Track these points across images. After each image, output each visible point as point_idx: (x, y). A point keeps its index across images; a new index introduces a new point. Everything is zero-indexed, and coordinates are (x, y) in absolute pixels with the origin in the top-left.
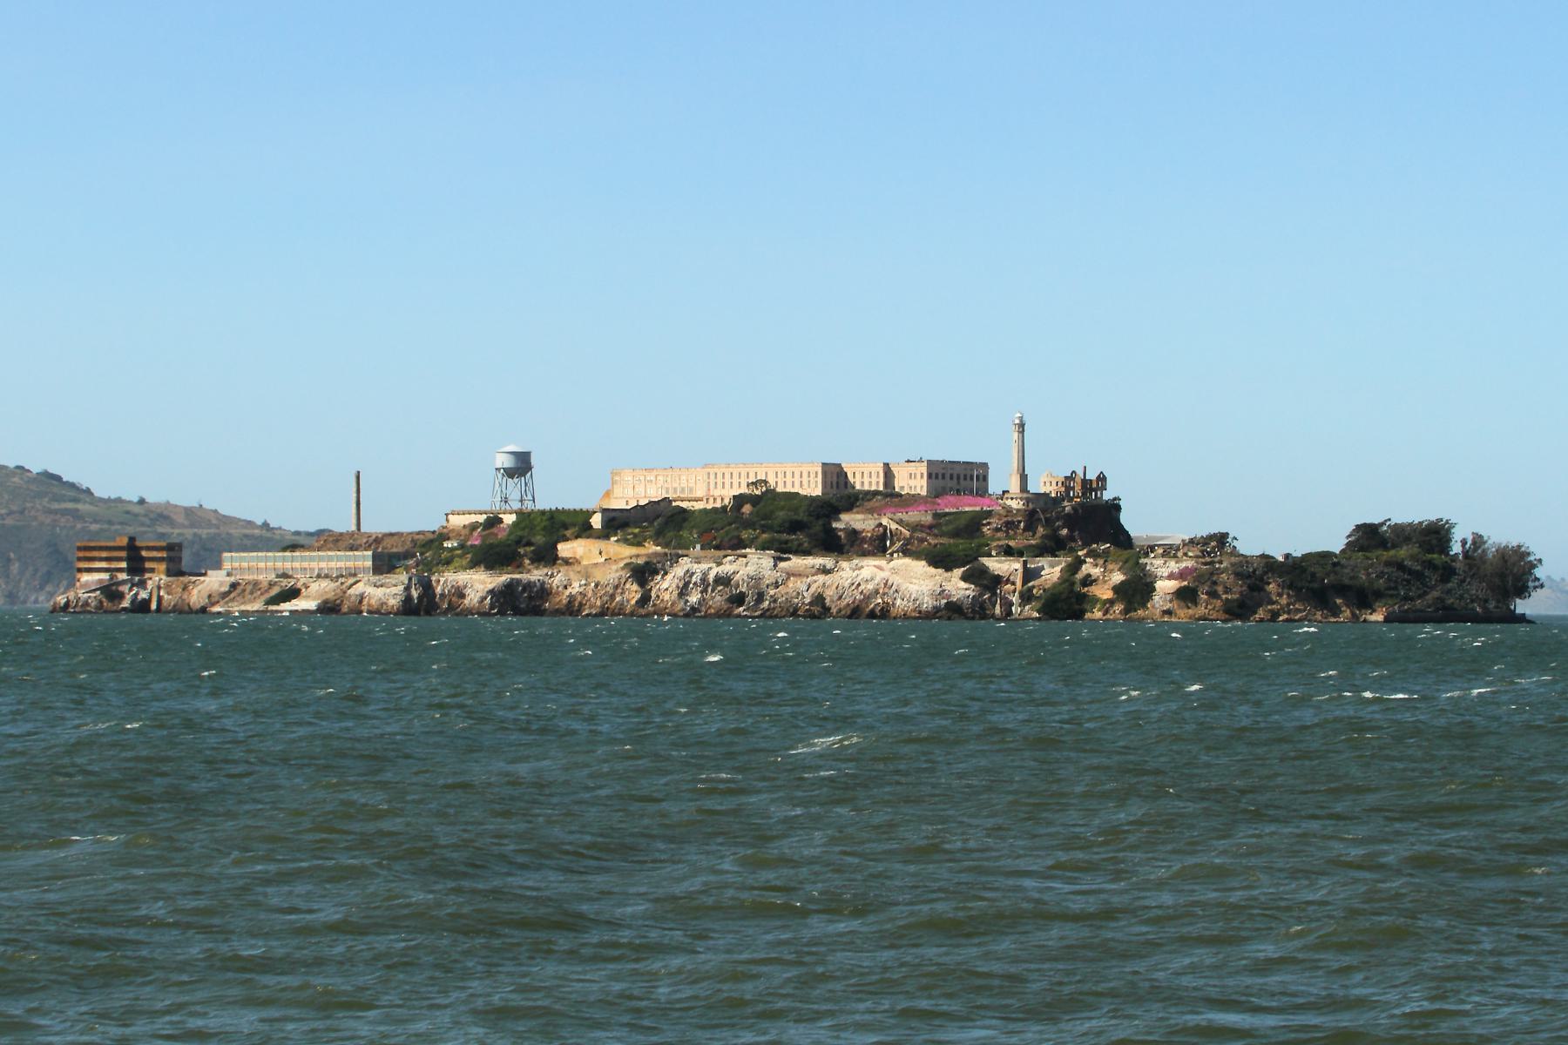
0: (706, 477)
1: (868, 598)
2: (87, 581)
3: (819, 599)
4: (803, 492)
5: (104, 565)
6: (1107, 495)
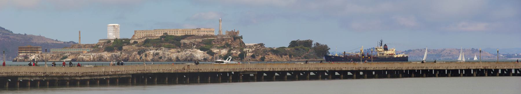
0: (154, 32)
1: (187, 57)
2: (21, 55)
3: (177, 58)
4: (174, 35)
5: (24, 52)
6: (239, 35)
